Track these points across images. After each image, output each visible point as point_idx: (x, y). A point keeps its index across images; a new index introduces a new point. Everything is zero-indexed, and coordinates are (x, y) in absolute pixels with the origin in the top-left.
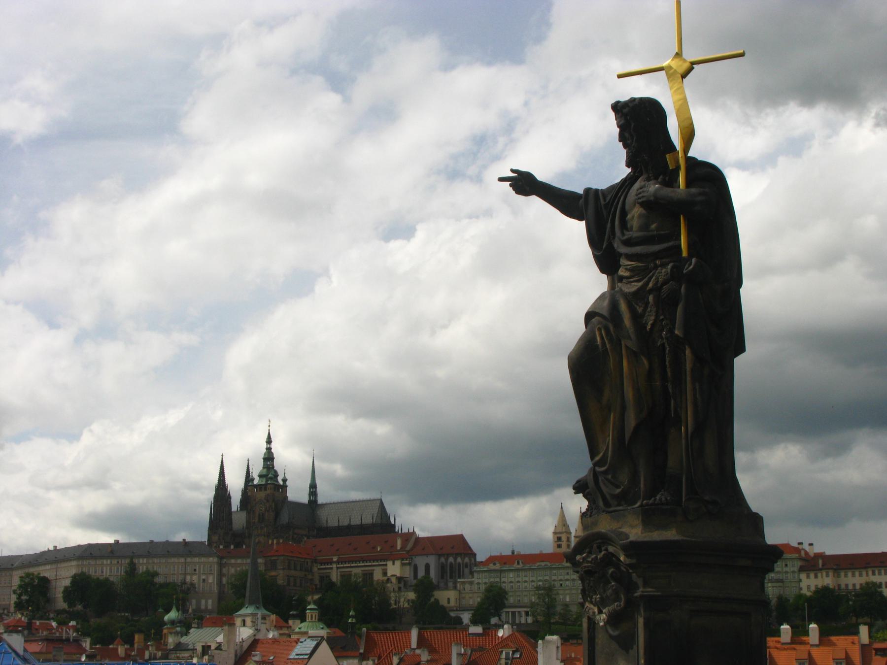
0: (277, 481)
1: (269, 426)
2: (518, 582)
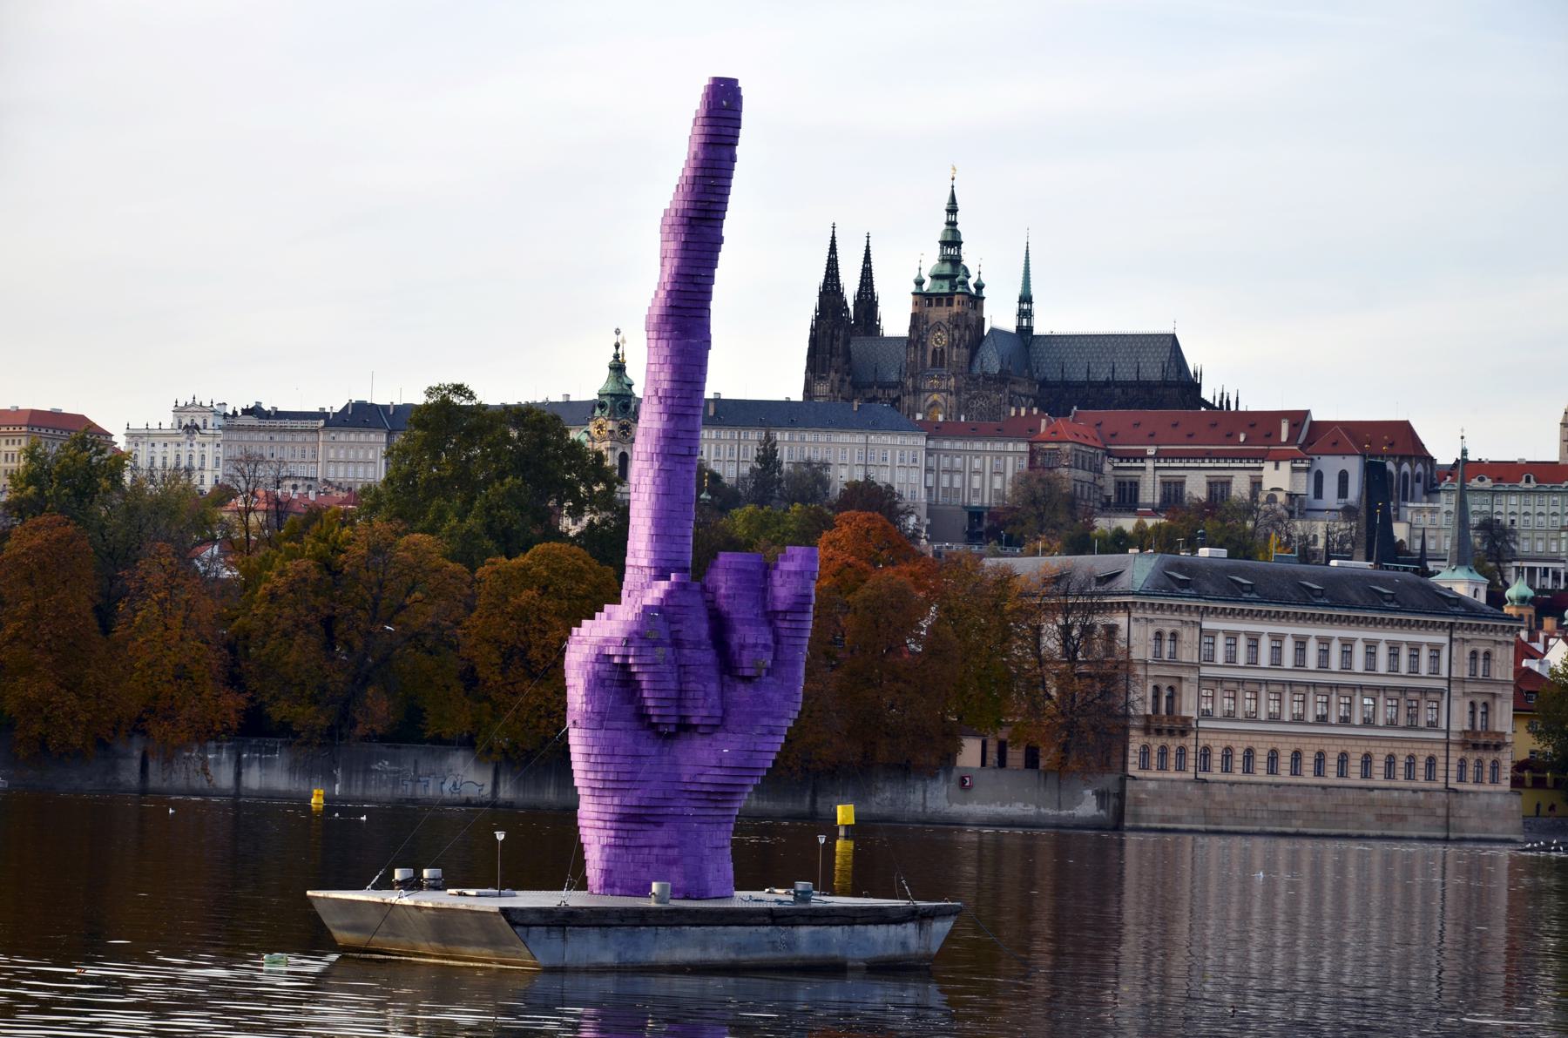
0: (969, 289)
1: (953, 179)
2: (1526, 514)
